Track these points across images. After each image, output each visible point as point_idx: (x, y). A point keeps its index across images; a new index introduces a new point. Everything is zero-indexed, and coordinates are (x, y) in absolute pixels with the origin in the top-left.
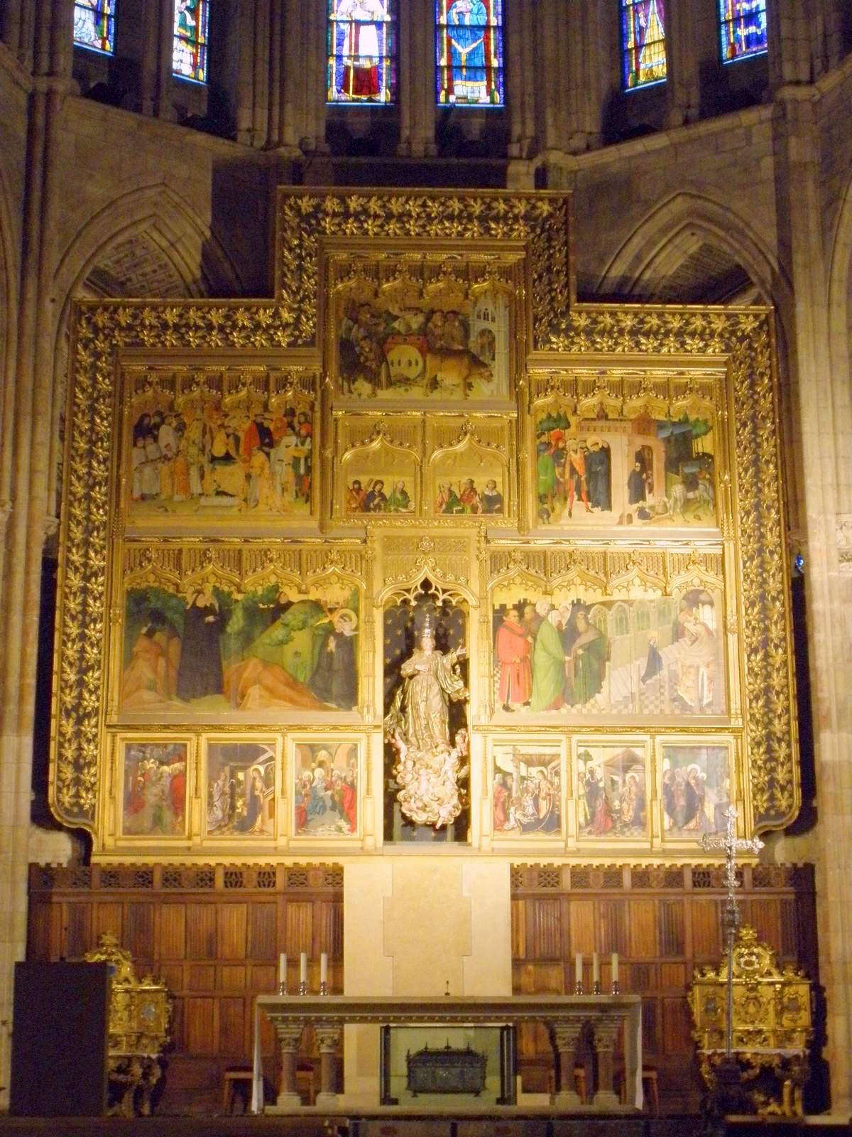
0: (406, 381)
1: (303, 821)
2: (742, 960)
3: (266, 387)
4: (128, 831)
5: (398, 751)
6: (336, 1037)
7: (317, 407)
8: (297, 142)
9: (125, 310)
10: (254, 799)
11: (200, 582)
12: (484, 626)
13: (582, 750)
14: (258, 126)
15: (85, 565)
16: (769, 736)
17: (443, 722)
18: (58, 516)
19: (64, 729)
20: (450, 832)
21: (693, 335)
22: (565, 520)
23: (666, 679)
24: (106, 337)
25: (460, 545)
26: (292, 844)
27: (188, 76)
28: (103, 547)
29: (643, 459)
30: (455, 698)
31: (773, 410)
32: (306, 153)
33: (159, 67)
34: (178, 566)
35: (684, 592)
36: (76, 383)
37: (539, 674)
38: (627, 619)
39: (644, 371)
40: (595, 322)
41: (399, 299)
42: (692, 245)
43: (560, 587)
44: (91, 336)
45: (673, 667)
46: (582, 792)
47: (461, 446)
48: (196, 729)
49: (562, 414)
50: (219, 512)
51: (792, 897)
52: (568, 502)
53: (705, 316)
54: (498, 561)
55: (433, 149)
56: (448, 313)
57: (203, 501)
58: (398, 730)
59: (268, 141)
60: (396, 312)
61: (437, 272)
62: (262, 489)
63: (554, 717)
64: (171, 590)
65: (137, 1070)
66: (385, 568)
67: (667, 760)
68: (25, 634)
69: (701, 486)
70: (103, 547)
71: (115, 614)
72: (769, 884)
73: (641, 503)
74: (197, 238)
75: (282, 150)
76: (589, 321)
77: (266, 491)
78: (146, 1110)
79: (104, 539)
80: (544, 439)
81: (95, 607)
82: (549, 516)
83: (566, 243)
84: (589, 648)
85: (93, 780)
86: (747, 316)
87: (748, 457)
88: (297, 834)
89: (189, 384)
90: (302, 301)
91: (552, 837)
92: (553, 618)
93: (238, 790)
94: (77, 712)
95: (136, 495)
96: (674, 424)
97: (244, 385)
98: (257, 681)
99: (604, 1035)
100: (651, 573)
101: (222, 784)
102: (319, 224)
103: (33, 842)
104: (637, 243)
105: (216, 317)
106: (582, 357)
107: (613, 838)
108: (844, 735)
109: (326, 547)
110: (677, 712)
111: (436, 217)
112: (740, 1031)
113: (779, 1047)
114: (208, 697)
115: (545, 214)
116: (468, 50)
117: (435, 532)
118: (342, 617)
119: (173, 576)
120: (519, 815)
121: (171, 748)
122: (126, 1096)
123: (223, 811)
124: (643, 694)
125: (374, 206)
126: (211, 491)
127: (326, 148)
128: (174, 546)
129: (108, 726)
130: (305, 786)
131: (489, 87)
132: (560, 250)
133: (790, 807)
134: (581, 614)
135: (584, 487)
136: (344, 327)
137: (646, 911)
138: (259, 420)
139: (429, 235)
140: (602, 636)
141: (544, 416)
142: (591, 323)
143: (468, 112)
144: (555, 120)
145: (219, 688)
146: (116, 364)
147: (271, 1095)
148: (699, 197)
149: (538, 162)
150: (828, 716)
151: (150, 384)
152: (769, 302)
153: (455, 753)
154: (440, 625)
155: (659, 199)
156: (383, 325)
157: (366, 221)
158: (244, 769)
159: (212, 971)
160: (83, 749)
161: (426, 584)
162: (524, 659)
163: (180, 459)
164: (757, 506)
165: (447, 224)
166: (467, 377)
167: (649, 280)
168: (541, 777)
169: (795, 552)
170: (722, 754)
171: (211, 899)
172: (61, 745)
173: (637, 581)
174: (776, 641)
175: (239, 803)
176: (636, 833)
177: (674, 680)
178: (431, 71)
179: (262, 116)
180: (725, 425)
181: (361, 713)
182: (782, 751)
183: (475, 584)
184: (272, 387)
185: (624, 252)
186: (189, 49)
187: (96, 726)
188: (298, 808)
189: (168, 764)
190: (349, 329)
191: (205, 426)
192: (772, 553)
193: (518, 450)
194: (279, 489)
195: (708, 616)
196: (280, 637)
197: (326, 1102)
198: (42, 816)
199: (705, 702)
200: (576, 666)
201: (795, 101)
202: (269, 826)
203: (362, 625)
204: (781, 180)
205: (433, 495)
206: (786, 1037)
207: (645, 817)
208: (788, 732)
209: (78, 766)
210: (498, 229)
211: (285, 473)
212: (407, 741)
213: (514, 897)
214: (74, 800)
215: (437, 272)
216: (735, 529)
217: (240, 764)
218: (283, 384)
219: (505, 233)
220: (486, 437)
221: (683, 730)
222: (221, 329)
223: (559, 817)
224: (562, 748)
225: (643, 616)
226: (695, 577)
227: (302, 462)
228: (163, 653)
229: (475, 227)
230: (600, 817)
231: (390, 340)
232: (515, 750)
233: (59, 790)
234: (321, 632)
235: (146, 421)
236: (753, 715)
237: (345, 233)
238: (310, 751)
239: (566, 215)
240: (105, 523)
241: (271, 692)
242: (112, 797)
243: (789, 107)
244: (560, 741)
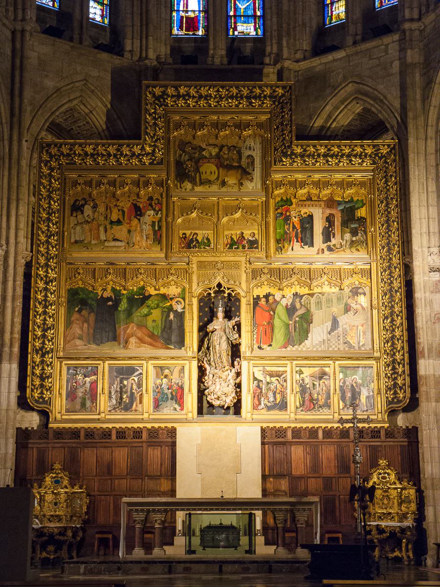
0: (209, 182)
1: (157, 406)
2: (380, 476)
3: (138, 186)
4: (67, 411)
5: (206, 369)
6: (163, 519)
7: (164, 196)
8: (155, 57)
9: (65, 146)
10: (132, 394)
11: (105, 285)
12: (248, 306)
13: (298, 369)
14: (135, 50)
15: (46, 276)
16: (394, 361)
17: (228, 355)
18: (32, 251)
19: (35, 360)
20: (232, 410)
21: (355, 156)
22: (290, 252)
23: (341, 333)
24: (56, 160)
25: (236, 265)
26: (151, 417)
27: (99, 22)
28: (55, 267)
29: (330, 220)
30: (234, 342)
31: (397, 194)
32: (160, 63)
33: (82, 18)
34: (94, 277)
35: (350, 288)
36: (41, 183)
37: (276, 331)
38: (321, 302)
39: (331, 175)
40: (305, 150)
41: (206, 140)
42: (358, 109)
43: (287, 286)
44: (48, 159)
45: (344, 326)
46: (298, 390)
47: (238, 215)
48: (103, 359)
49: (288, 198)
50: (114, 249)
51: (406, 444)
52: (292, 243)
53: (362, 146)
54: (255, 274)
55: (225, 60)
56: (231, 147)
57: (106, 244)
58: (206, 359)
59: (140, 57)
60: (204, 146)
61: (225, 125)
62: (136, 238)
64: (90, 289)
65: (70, 533)
66: (198, 278)
67: (341, 374)
68: (13, 312)
69: (359, 234)
70: (55, 267)
71: (62, 301)
72: (394, 437)
73: (329, 243)
74: (103, 108)
75: (147, 61)
76: (302, 150)
77: (138, 238)
78: (74, 554)
79: (56, 263)
80: (279, 211)
81: (52, 298)
82: (281, 250)
83: (290, 110)
84: (302, 317)
85: (50, 385)
86: (384, 145)
87: (384, 219)
88: (154, 412)
89: (99, 184)
90: (156, 141)
91: (283, 413)
92: (284, 302)
93: (124, 390)
94: (42, 351)
95: (73, 240)
96: (346, 202)
97: (127, 184)
99: (302, 517)
100: (334, 279)
101: (116, 386)
102: (165, 101)
103: (18, 417)
104: (329, 108)
105: (112, 150)
106: (299, 169)
107: (314, 413)
108: (431, 361)
109: (168, 267)
110: (347, 349)
111: (224, 97)
112: (379, 513)
113: (400, 522)
114: (109, 343)
115: (280, 94)
116: (244, 7)
117: (223, 259)
118: (176, 302)
119: (91, 281)
120: (266, 401)
121: (90, 369)
122: (64, 547)
123: (117, 401)
124: (329, 340)
125: (192, 92)
126: (111, 239)
127: (170, 60)
128: (92, 266)
129: (58, 358)
130: (158, 388)
131: (255, 26)
132: (287, 113)
133: (404, 397)
134: (298, 300)
135: (300, 235)
136: (177, 155)
137: (330, 451)
138: (134, 202)
139: (221, 106)
140: (308, 311)
141: (280, 199)
142: (303, 151)
143: (245, 39)
144: (287, 44)
145: (115, 338)
146: (62, 174)
147: (130, 548)
148: (360, 83)
149: (278, 66)
150: (422, 352)
151: (79, 184)
152: (395, 138)
153: (234, 370)
154: (227, 305)
155: (340, 84)
156: (198, 153)
157: (188, 100)
158: (127, 379)
159: (109, 482)
160: (45, 370)
161: (219, 285)
162: (269, 323)
163: (94, 222)
164: (388, 244)
165: (230, 101)
166: (241, 179)
167: (335, 127)
168: (277, 382)
169: (408, 269)
170: (370, 370)
171: (110, 445)
172: (33, 368)
173: (326, 283)
174: (398, 313)
175: (125, 396)
176: (325, 411)
177: (345, 334)
178: (224, 19)
179: (137, 43)
180: (372, 202)
181: (186, 350)
182: (400, 370)
183: (244, 285)
184: (141, 186)
185: (322, 113)
186: (99, 7)
187: (52, 358)
188: (154, 398)
189: (89, 377)
190: (181, 155)
191: (107, 205)
192: (395, 268)
193: (266, 217)
194: (145, 237)
195: (363, 300)
196: (145, 312)
197: (157, 552)
198: (23, 403)
199: (361, 344)
200: (295, 326)
201: (411, 30)
202: (140, 408)
203: (187, 306)
204: (403, 73)
205: (223, 241)
206: (404, 517)
207: (330, 402)
208: (403, 359)
209: (42, 378)
210: (256, 103)
211: (147, 229)
212: (210, 364)
213: (263, 444)
214: (40, 395)
215: (225, 125)
216: (376, 256)
217: (126, 376)
218: (147, 184)
219: (259, 105)
220: (249, 210)
221: (349, 358)
222: (115, 156)
223: (286, 403)
224: (288, 368)
225: (329, 301)
226: (356, 280)
227: (157, 223)
229: (244, 102)
230: (307, 403)
231: (201, 161)
232: (264, 369)
233: (32, 390)
234: (166, 310)
235: (77, 203)
236: (385, 351)
237: (178, 106)
239: (290, 95)
240: (56, 255)
241: (141, 340)
242: (60, 394)
243: (407, 33)
244: (287, 364)
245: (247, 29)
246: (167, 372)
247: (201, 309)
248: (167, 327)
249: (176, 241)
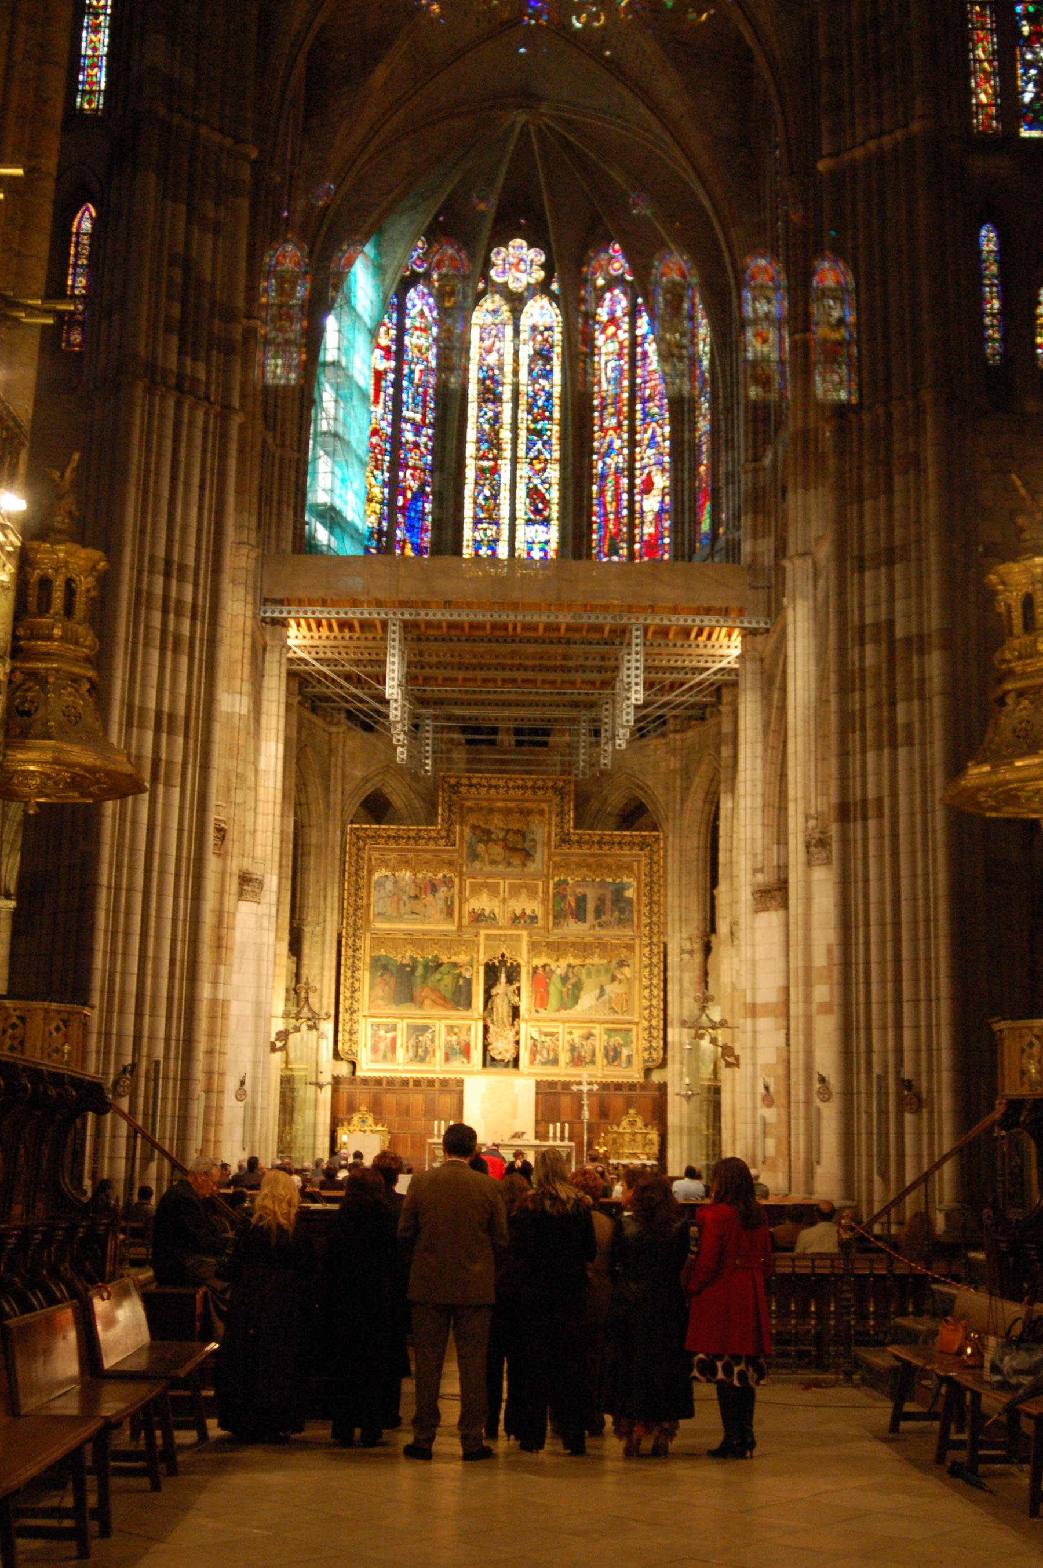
1: (447, 1058)
22: (565, 927)
29: (601, 900)
62: (430, 911)
63: (557, 1015)
66: (486, 946)
81: (358, 963)
92: (559, 971)
98: (426, 998)
101: (412, 1042)
140: (579, 980)
153: (514, 1031)
161: (503, 956)
183: (525, 955)
195: (626, 970)
198: (336, 1055)
209: (351, 1033)
211: (441, 903)
228: (387, 984)
229: (529, 791)
238: (450, 1029)
241: (434, 1001)
246: (456, 1030)
247: (486, 973)
249: (466, 914)
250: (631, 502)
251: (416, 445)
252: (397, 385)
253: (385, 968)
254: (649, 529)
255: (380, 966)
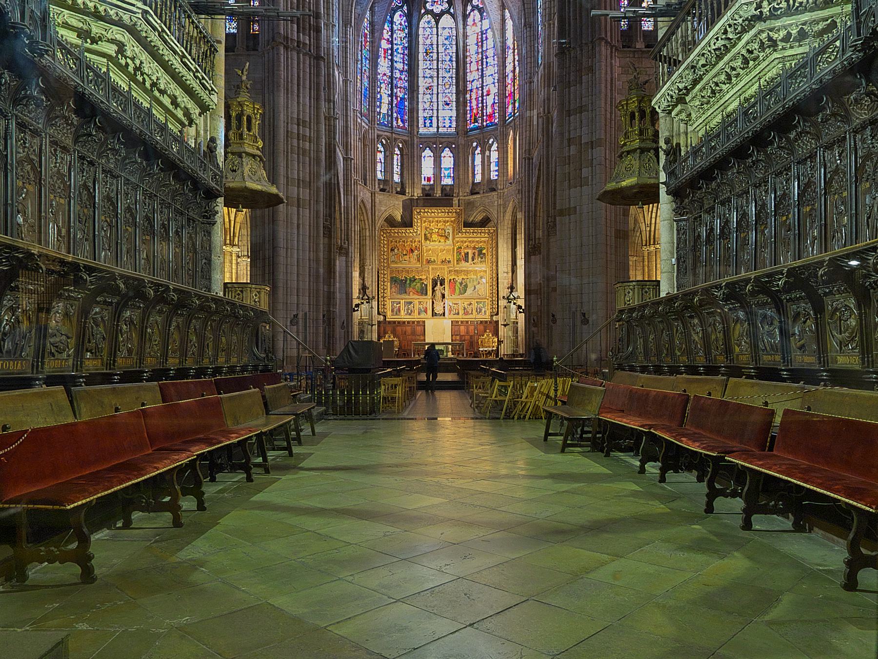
1: (419, 314)
29: (474, 254)
61: (440, 222)
62: (412, 260)
63: (458, 297)
89: (399, 242)
147: (414, 356)
195: (484, 280)
198: (379, 313)
218: (415, 242)
226: (482, 274)
228: (396, 287)
238: (420, 303)
245: (448, 181)
248: (422, 289)
250: (482, 100)
251: (400, 79)
252: (392, 55)
253: (395, 281)
254: (489, 110)
255: (394, 280)
